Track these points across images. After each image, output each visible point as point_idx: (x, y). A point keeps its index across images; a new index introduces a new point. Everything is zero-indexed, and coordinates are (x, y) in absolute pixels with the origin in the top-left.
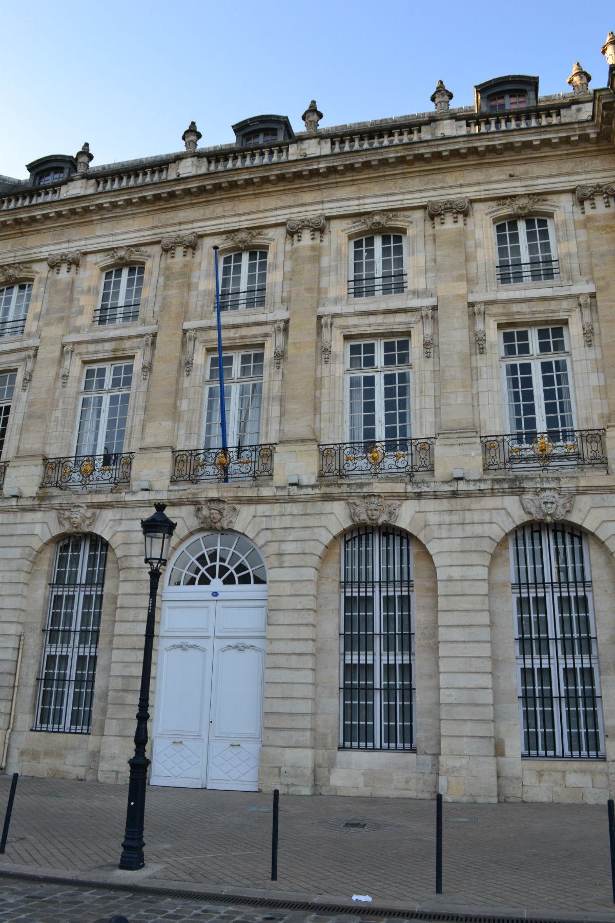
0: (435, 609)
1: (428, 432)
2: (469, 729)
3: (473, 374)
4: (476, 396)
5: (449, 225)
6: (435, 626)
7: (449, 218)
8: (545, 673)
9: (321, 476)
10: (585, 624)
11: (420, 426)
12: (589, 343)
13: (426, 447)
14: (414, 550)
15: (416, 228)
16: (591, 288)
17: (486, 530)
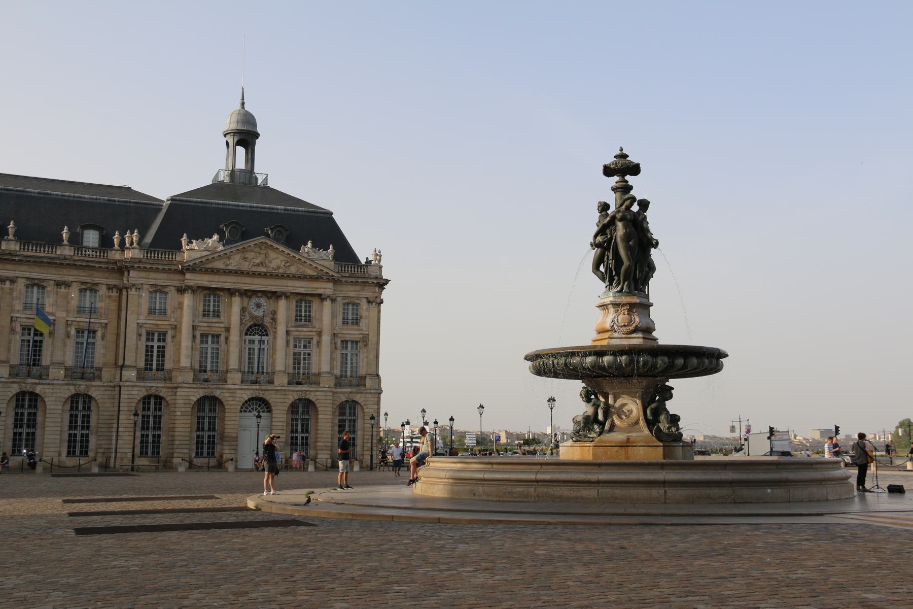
0: (45, 418)
1: (48, 363)
2: (52, 449)
3: (65, 345)
4: (65, 353)
5: (63, 290)
6: (44, 421)
7: (63, 287)
8: (75, 435)
9: (10, 375)
10: (88, 422)
11: (46, 360)
12: (103, 339)
13: (47, 368)
14: (39, 400)
15: (50, 287)
16: (106, 321)
17: (63, 395)
